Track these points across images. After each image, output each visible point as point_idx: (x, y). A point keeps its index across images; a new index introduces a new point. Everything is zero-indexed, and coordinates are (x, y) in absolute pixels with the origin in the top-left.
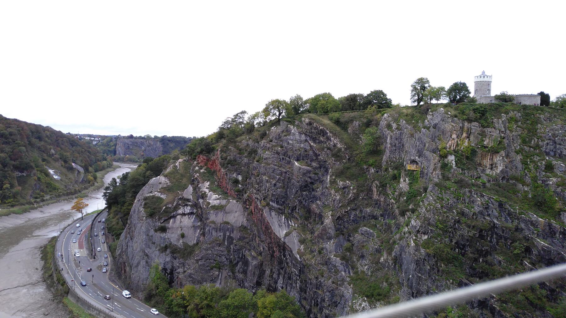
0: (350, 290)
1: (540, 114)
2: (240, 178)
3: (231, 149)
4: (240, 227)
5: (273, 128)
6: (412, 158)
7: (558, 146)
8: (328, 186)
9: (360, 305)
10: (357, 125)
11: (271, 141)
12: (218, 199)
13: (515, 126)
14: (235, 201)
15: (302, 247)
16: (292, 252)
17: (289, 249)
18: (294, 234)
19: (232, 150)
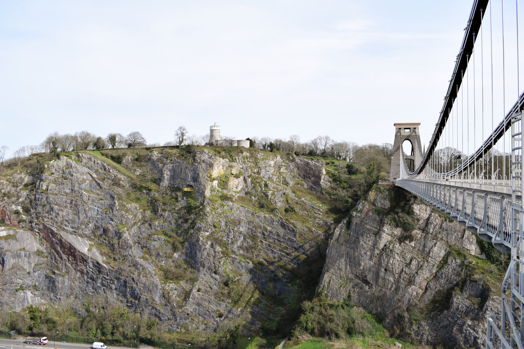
0: (157, 279)
1: (258, 154)
2: (20, 208)
3: (3, 183)
4: (36, 252)
5: (51, 162)
6: (188, 183)
7: (268, 173)
8: (117, 208)
9: (169, 286)
10: (130, 159)
11: (53, 174)
12: (3, 230)
13: (246, 161)
14: (22, 231)
15: (105, 258)
16: (98, 263)
17: (95, 261)
18: (94, 250)
19: (5, 183)
